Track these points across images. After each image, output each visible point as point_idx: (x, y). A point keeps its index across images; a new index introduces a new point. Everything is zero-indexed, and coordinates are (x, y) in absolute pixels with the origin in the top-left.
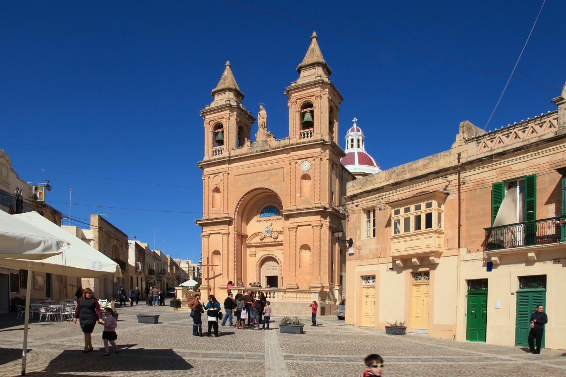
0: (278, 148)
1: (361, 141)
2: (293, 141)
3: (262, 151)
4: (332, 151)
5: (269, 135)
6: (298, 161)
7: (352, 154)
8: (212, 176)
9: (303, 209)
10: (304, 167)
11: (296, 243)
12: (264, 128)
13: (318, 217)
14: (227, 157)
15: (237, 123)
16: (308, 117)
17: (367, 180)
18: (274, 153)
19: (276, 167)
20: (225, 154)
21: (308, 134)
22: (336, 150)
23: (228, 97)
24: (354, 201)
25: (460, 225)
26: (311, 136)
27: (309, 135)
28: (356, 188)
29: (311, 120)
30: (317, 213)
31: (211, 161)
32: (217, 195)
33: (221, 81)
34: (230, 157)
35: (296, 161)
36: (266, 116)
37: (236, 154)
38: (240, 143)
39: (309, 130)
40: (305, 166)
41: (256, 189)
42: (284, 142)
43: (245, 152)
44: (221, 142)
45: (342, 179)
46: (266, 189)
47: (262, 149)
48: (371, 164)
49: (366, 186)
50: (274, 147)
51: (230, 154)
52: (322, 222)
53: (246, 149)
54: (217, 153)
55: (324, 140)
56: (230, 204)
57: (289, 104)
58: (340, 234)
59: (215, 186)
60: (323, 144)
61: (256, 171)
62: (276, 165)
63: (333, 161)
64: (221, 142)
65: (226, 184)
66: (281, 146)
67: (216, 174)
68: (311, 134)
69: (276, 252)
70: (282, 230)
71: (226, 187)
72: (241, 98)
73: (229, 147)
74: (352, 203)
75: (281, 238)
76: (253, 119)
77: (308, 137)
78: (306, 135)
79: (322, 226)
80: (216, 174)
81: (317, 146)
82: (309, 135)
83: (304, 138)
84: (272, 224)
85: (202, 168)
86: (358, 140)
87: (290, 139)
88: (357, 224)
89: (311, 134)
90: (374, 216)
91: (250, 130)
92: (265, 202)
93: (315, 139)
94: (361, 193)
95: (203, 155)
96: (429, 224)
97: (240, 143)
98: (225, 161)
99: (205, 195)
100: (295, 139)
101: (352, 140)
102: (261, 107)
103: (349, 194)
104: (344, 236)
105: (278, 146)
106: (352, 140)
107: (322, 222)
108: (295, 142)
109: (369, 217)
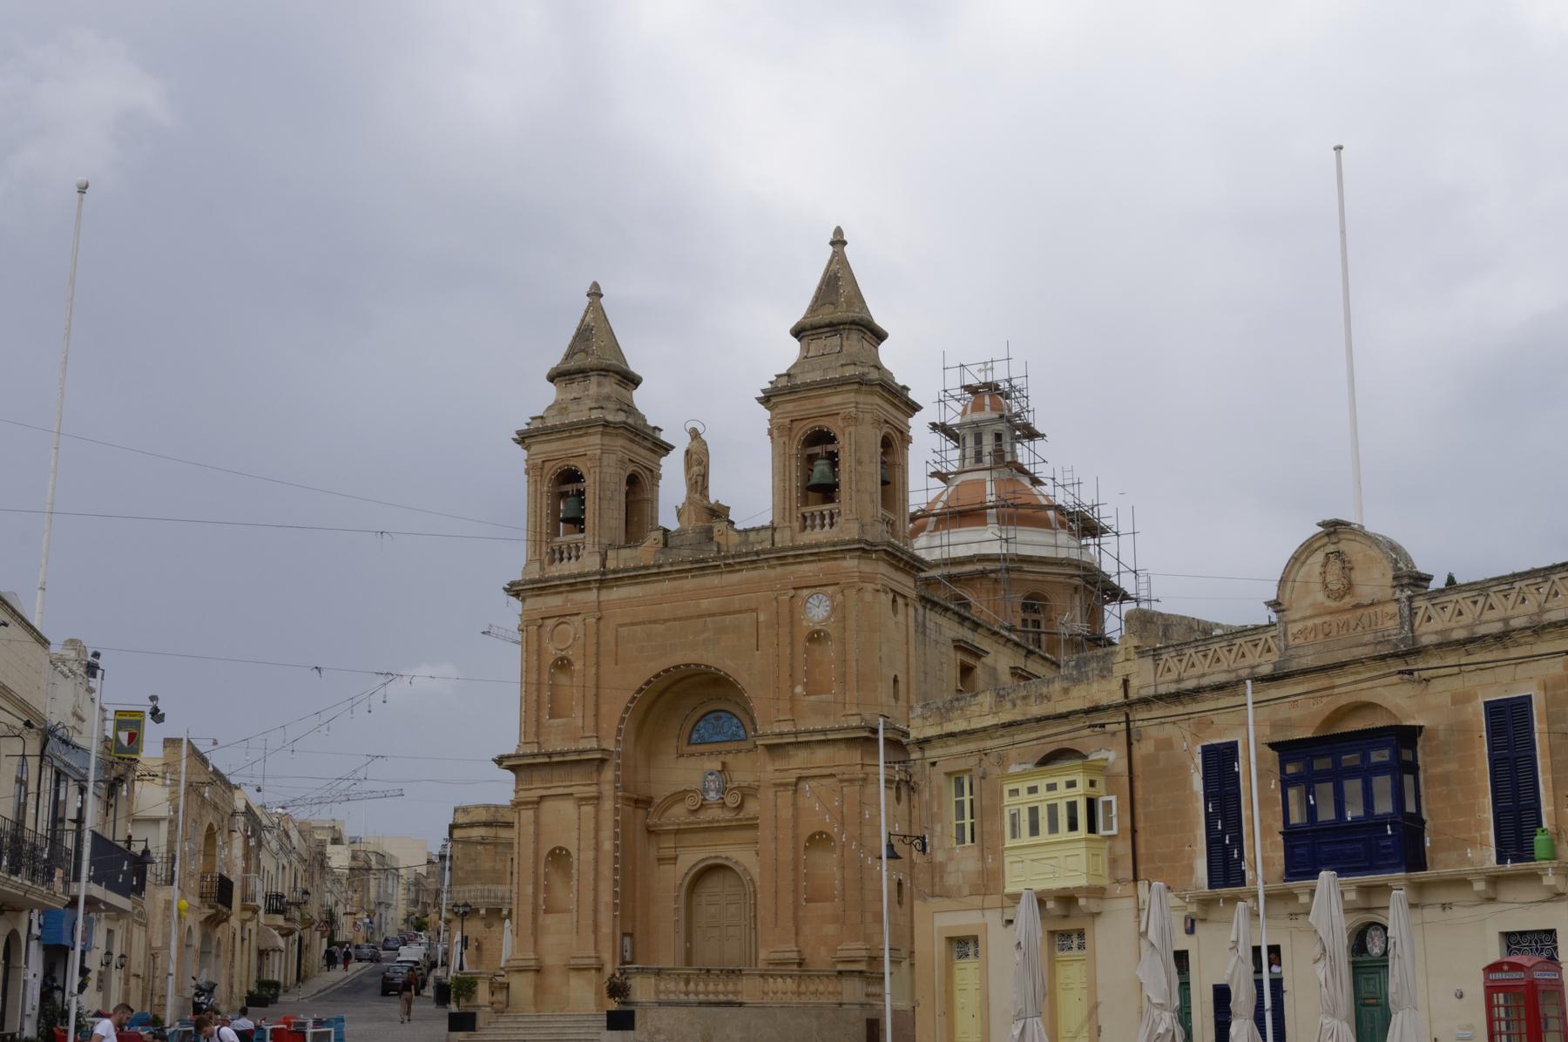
0: (739, 556)
8: (550, 623)
9: (815, 732)
10: (815, 611)
14: (595, 573)
19: (737, 607)
20: (589, 563)
21: (823, 517)
25: (1134, 831)
26: (832, 525)
27: (827, 521)
30: (849, 741)
32: (563, 679)
34: (604, 574)
45: (924, 633)
53: (645, 553)
54: (565, 555)
56: (604, 709)
60: (864, 550)
61: (679, 613)
65: (592, 649)
67: (563, 617)
71: (593, 660)
77: (823, 526)
80: (563, 617)
82: (827, 521)
83: (813, 527)
84: (724, 764)
91: (659, 477)
94: (940, 737)
96: (1073, 826)
100: (788, 533)
103: (914, 734)
109: (960, 792)
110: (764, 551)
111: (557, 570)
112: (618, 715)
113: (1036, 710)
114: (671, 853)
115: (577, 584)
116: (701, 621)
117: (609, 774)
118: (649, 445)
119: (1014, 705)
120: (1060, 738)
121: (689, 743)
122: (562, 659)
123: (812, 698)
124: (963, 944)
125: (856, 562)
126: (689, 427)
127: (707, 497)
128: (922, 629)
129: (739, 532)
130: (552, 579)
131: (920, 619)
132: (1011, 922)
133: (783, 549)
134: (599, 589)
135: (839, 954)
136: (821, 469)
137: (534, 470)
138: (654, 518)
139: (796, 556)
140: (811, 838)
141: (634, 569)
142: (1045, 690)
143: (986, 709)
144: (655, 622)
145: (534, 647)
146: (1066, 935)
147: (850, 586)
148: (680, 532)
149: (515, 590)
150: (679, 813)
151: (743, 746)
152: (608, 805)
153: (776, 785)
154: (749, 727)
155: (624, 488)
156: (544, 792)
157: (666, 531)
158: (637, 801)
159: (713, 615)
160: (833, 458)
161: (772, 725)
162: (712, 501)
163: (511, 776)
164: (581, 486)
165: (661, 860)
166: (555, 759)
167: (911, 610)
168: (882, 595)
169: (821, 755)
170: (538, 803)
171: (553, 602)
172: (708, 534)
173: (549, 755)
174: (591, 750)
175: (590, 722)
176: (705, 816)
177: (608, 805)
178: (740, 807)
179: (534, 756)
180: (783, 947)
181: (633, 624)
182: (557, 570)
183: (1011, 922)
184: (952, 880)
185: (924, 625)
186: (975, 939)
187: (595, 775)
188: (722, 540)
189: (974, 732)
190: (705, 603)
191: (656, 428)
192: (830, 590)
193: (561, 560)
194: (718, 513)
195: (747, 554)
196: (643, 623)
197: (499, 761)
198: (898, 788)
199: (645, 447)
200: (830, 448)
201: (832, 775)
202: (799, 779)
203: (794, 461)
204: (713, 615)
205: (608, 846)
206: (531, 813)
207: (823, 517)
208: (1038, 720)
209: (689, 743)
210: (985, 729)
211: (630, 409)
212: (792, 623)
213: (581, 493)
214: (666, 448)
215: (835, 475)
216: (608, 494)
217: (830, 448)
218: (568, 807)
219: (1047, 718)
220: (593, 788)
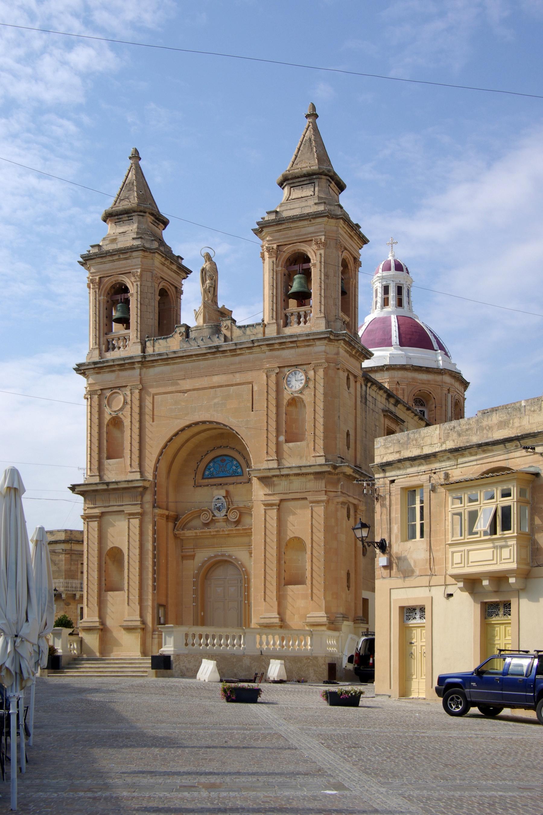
13: (321, 484)
19: (238, 381)
20: (133, 350)
21: (299, 317)
22: (354, 348)
26: (305, 322)
32: (116, 433)
37: (157, 351)
41: (197, 424)
46: (218, 423)
53: (174, 343)
59: (114, 414)
71: (136, 417)
77: (299, 323)
81: (318, 343)
89: (305, 317)
98: (133, 363)
100: (275, 327)
108: (275, 335)
110: (258, 340)
111: (110, 355)
115: (125, 364)
116: (213, 390)
117: (148, 497)
118: (174, 267)
123: (291, 444)
125: (323, 348)
126: (204, 252)
127: (216, 303)
129: (240, 327)
130: (107, 361)
134: (141, 369)
137: (97, 284)
138: (178, 321)
139: (281, 343)
145: (96, 409)
148: (198, 328)
149: (81, 369)
152: (148, 519)
154: (244, 465)
155: (158, 298)
156: (104, 510)
157: (188, 328)
158: (168, 517)
159: (221, 386)
162: (220, 305)
163: (81, 498)
164: (126, 296)
165: (184, 558)
168: (341, 372)
171: (109, 378)
172: (217, 330)
177: (148, 519)
179: (96, 484)
182: (110, 355)
187: (139, 498)
188: (228, 334)
191: (179, 257)
192: (305, 367)
194: (225, 314)
197: (73, 488)
199: (171, 270)
201: (306, 499)
204: (221, 386)
207: (299, 317)
211: (162, 242)
212: (279, 391)
213: (127, 302)
214: (187, 272)
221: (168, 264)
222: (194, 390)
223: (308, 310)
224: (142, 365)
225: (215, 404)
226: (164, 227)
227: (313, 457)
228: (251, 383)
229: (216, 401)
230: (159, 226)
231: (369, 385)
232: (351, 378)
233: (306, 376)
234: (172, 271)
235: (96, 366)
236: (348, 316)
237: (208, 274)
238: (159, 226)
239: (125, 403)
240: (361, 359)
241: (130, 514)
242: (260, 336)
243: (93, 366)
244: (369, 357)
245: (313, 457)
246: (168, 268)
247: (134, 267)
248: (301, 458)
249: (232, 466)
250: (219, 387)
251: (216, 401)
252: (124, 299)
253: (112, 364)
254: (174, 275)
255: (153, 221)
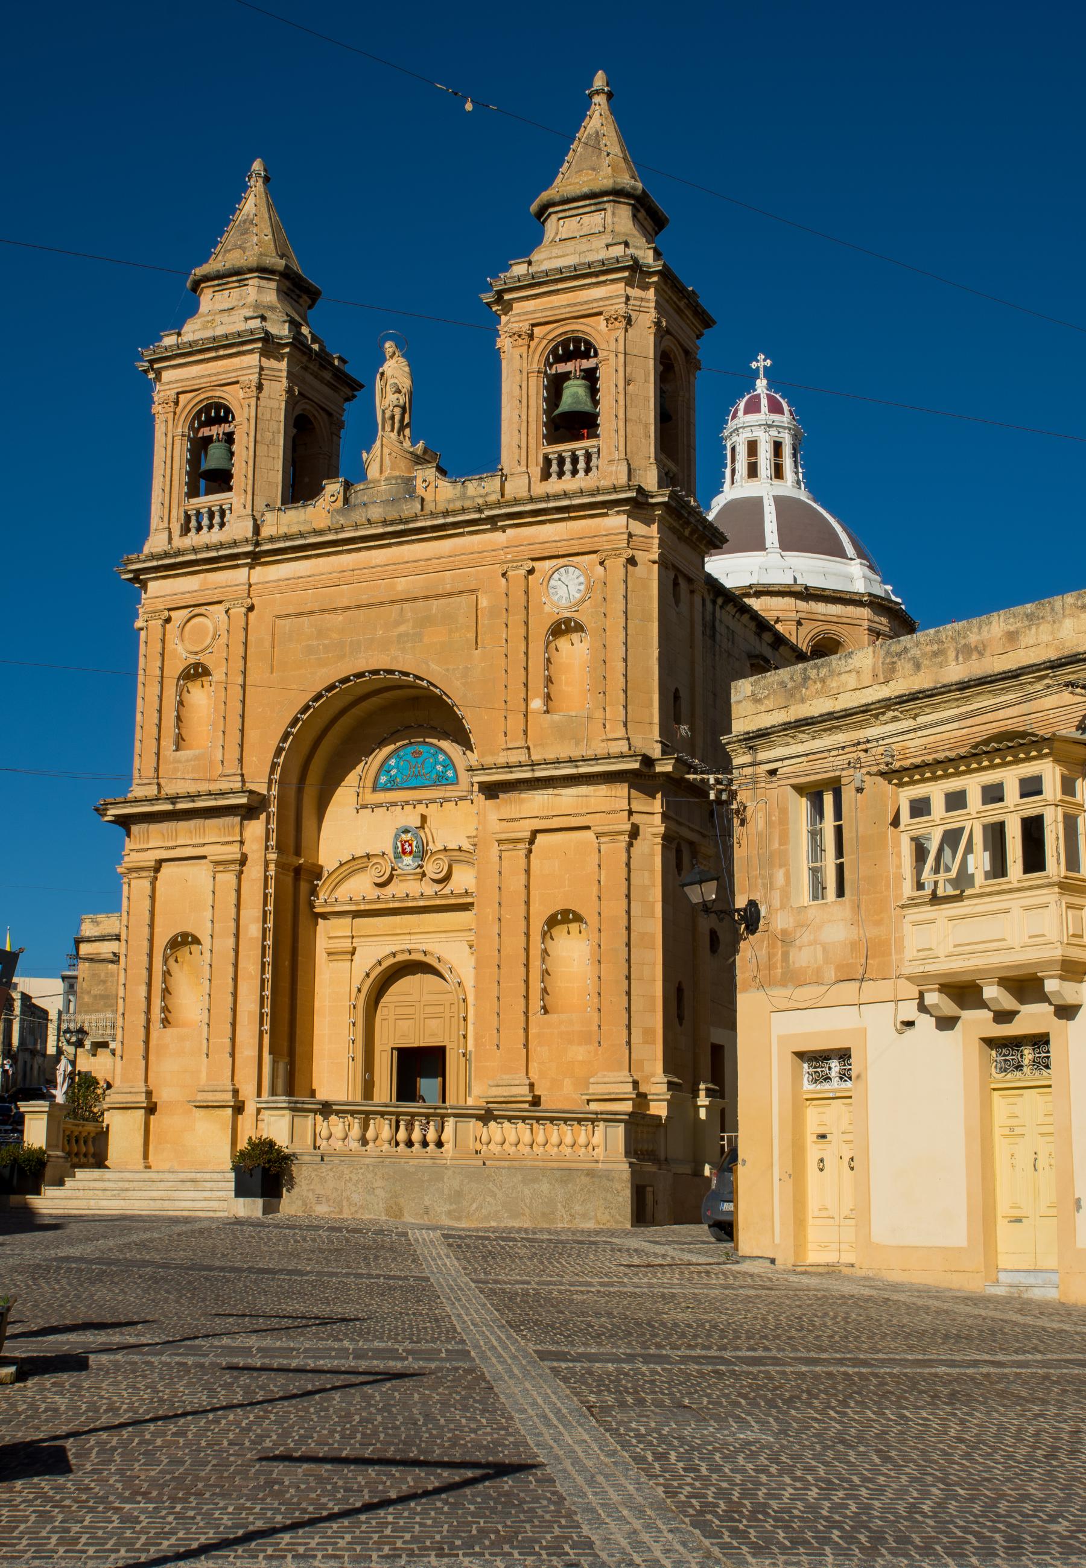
0: (454, 513)
1: (787, 451)
2: (516, 487)
3: (392, 523)
4: (672, 529)
5: (419, 460)
6: (536, 564)
7: (755, 505)
8: (178, 616)
10: (562, 591)
11: (527, 903)
12: (402, 428)
15: (292, 400)
16: (574, 394)
17: (806, 679)
18: (440, 531)
19: (448, 588)
20: (238, 528)
21: (575, 460)
22: (688, 523)
23: (257, 305)
24: (762, 756)
26: (588, 470)
27: (581, 465)
28: (769, 704)
29: (587, 407)
31: (179, 553)
32: (199, 696)
33: (231, 237)
35: (531, 564)
36: (406, 383)
37: (283, 530)
38: (300, 487)
39: (579, 446)
40: (565, 589)
42: (482, 490)
43: (322, 523)
44: (221, 480)
45: (713, 637)
47: (393, 515)
48: (836, 550)
49: (803, 701)
50: (441, 507)
51: (257, 530)
52: (636, 818)
53: (318, 514)
54: (205, 522)
55: (640, 490)
56: (252, 735)
57: (504, 343)
58: (709, 892)
59: (192, 660)
61: (364, 599)
62: (448, 581)
63: (674, 567)
64: (221, 480)
66: (468, 504)
67: (197, 607)
68: (588, 457)
69: (445, 941)
70: (466, 846)
72: (305, 299)
73: (252, 498)
74: (754, 764)
75: (463, 879)
76: (351, 386)
77: (574, 472)
78: (568, 466)
79: (634, 833)
80: (197, 607)
84: (424, 818)
85: (139, 579)
86: (778, 446)
87: (504, 479)
88: (776, 845)
89: (588, 457)
90: (838, 815)
91: (341, 425)
92: (383, 717)
93: (604, 483)
95: (143, 532)
96: (1034, 860)
97: (300, 487)
99: (147, 694)
101: (752, 447)
102: (389, 347)
104: (727, 890)
105: (458, 505)
106: (752, 447)
107: (636, 818)
112: (274, 743)
113: (955, 672)
114: (346, 945)
116: (396, 608)
118: (327, 375)
119: (918, 666)
120: (1001, 714)
121: (374, 789)
122: (196, 665)
123: (556, 717)
124: (824, 1060)
128: (711, 629)
131: (708, 618)
132: (910, 1024)
133: (516, 502)
135: (593, 1089)
136: (574, 394)
140: (552, 922)
141: (301, 535)
142: (973, 638)
143: (867, 679)
144: (329, 611)
146: (1014, 1043)
147: (615, 552)
150: (360, 888)
151: (452, 792)
152: (254, 872)
153: (500, 842)
159: (414, 599)
160: (591, 377)
161: (495, 746)
166: (180, 806)
167: (698, 600)
169: (569, 798)
170: (157, 870)
173: (173, 799)
174: (233, 792)
175: (234, 753)
176: (397, 889)
178: (447, 879)
180: (507, 1078)
181: (297, 615)
183: (910, 1024)
184: (803, 957)
185: (714, 627)
186: (844, 1055)
189: (847, 714)
190: (402, 585)
193: (199, 528)
195: (463, 510)
196: (312, 613)
198: (679, 851)
199: (321, 380)
200: (587, 364)
202: (535, 833)
203: (533, 381)
204: (414, 599)
205: (252, 929)
206: (146, 884)
208: (963, 686)
209: (374, 789)
210: (865, 709)
213: (229, 438)
215: (596, 403)
216: (268, 436)
217: (587, 364)
218: (200, 873)
219: (983, 681)
220: (236, 848)
221: (316, 369)
222: (358, 607)
223: (594, 447)
224: (253, 560)
225: (400, 636)
226: (310, 302)
227: (603, 741)
228: (477, 590)
229: (402, 629)
230: (301, 301)
231: (720, 601)
232: (681, 581)
233: (588, 578)
234: (322, 382)
235: (160, 563)
236: (675, 461)
237: (390, 381)
238: (301, 301)
239: (216, 636)
240: (702, 547)
241: (218, 863)
242: (494, 498)
243: (155, 563)
244: (718, 543)
245: (603, 741)
246: (316, 377)
247: (245, 372)
248: (577, 744)
249: (436, 764)
250: (408, 600)
251: (402, 629)
252: (224, 434)
253: (193, 557)
254: (327, 390)
255: (289, 289)
